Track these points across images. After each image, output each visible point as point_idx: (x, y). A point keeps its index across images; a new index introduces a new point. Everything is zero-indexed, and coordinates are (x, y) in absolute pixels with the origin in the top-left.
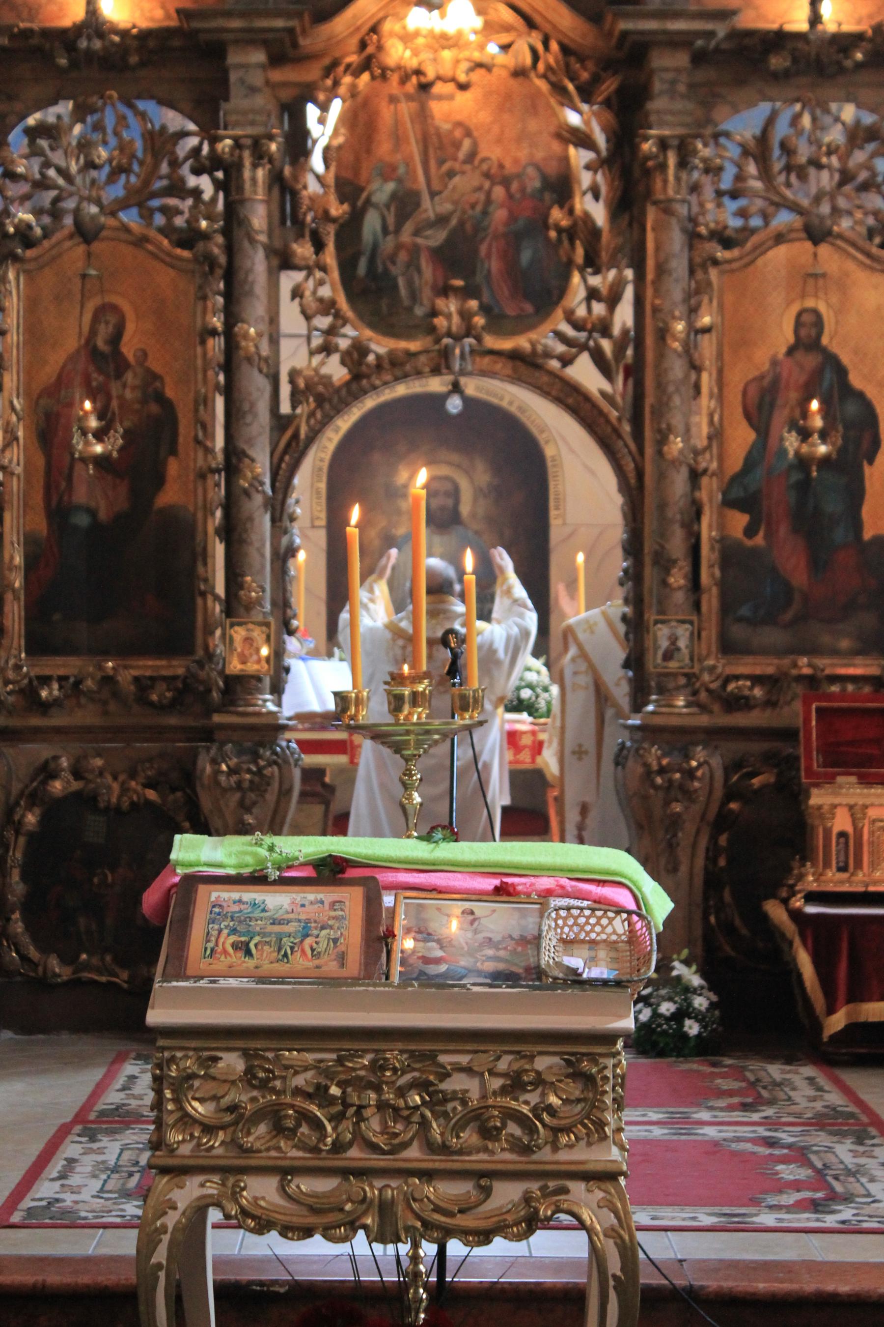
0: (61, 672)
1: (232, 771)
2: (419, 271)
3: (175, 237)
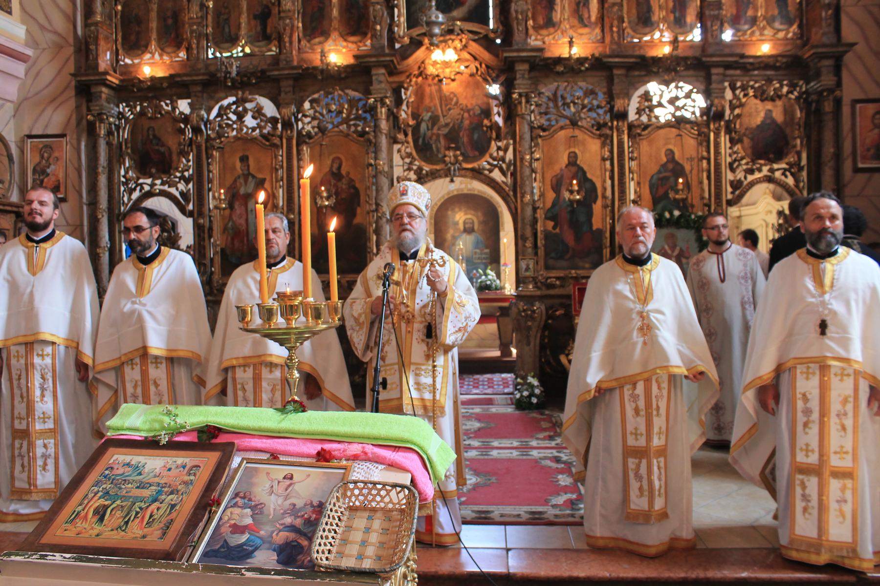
2: (440, 142)
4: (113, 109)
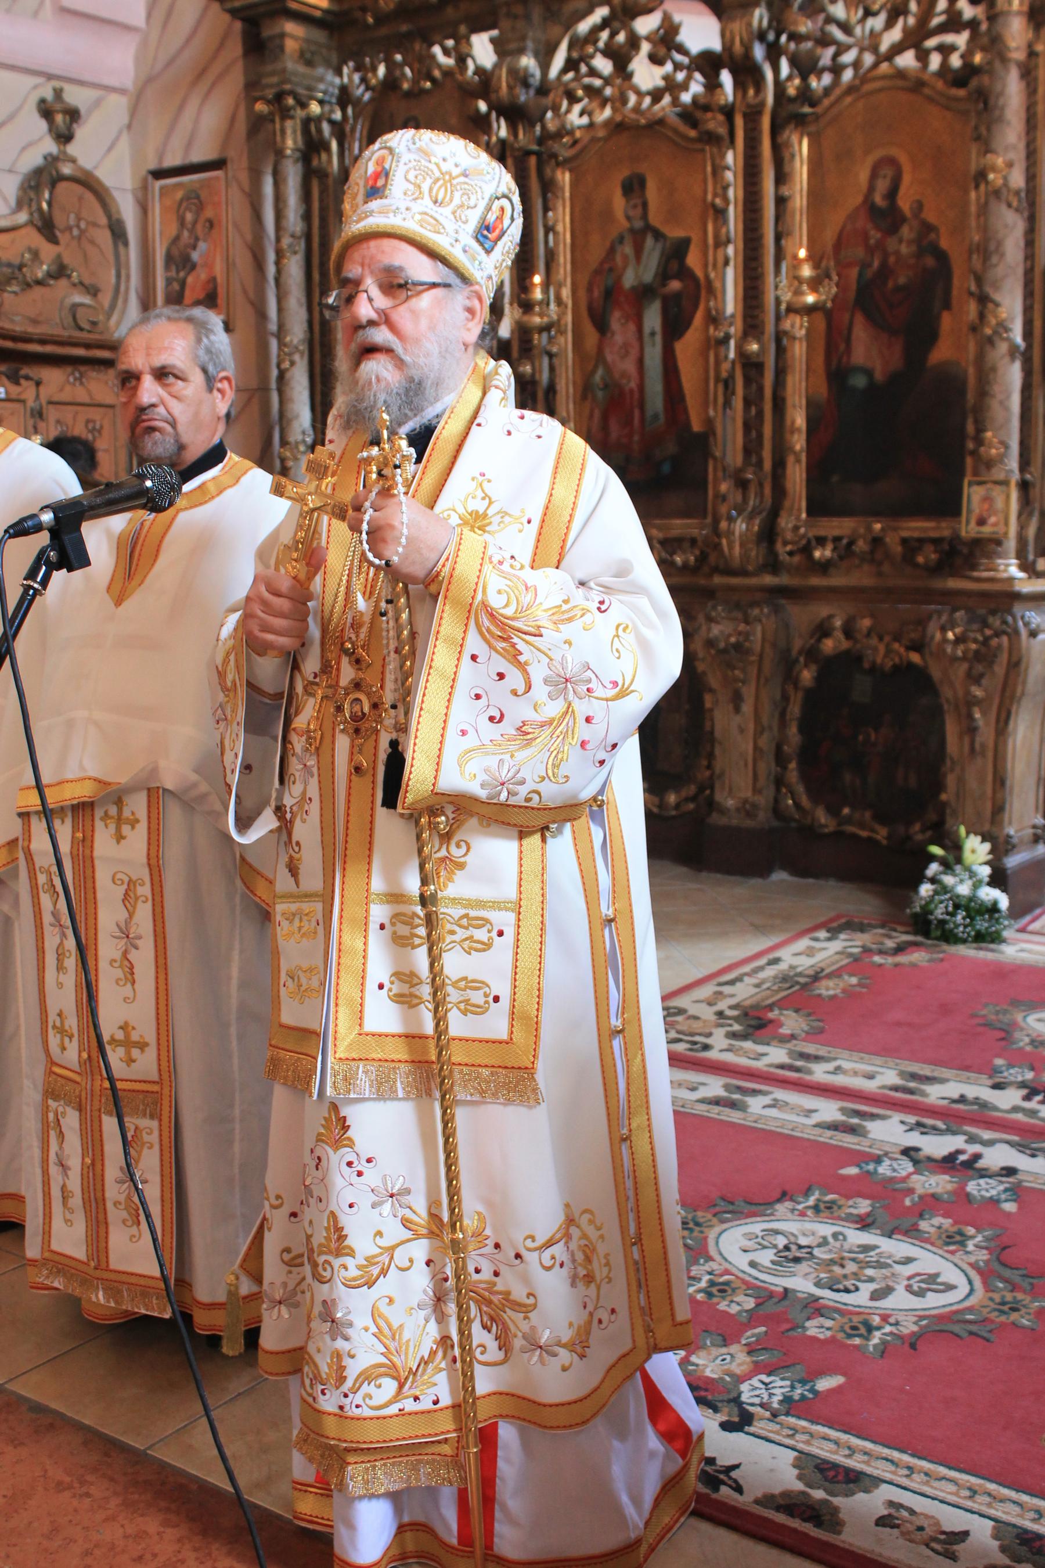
0: (837, 532)
1: (959, 640)
3: (950, 77)
4: (321, 79)
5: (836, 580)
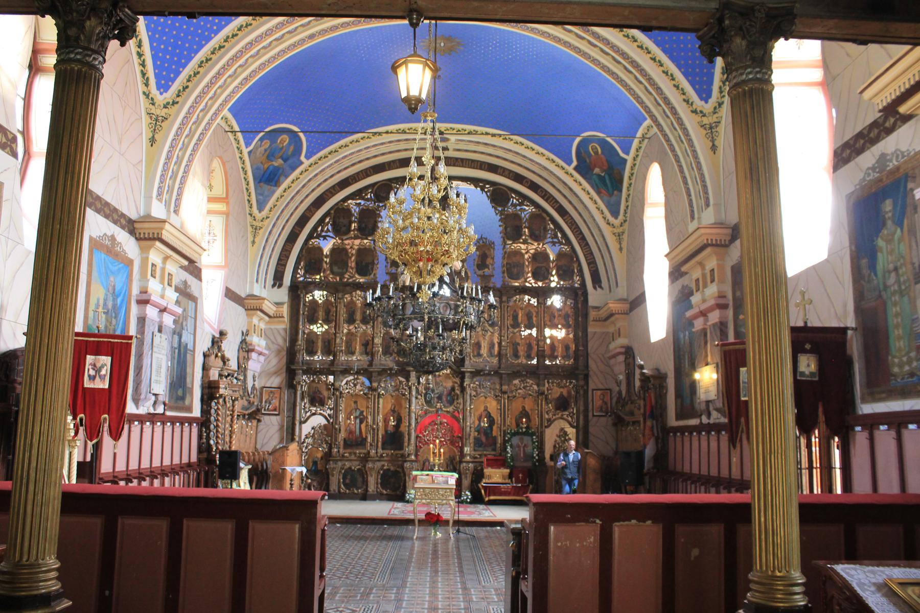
5: (385, 459)
